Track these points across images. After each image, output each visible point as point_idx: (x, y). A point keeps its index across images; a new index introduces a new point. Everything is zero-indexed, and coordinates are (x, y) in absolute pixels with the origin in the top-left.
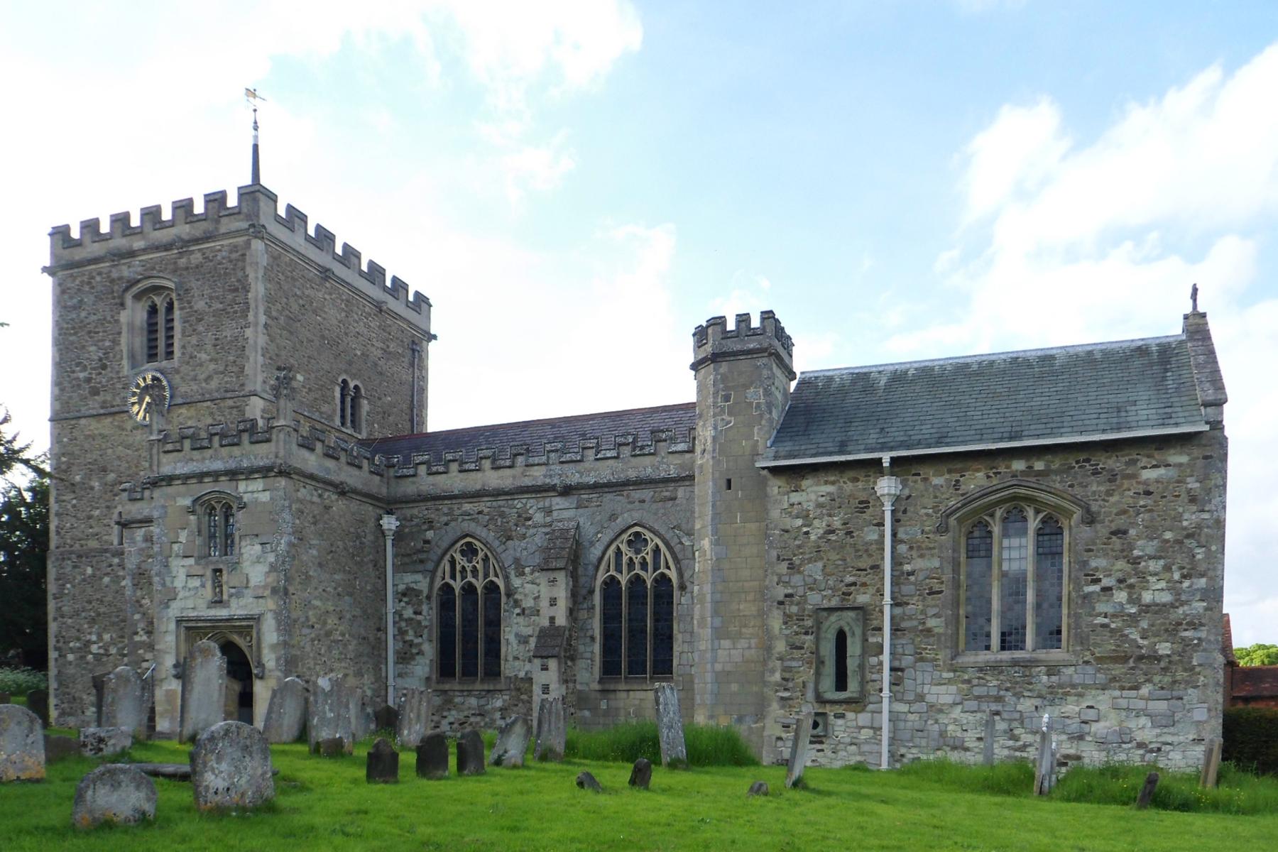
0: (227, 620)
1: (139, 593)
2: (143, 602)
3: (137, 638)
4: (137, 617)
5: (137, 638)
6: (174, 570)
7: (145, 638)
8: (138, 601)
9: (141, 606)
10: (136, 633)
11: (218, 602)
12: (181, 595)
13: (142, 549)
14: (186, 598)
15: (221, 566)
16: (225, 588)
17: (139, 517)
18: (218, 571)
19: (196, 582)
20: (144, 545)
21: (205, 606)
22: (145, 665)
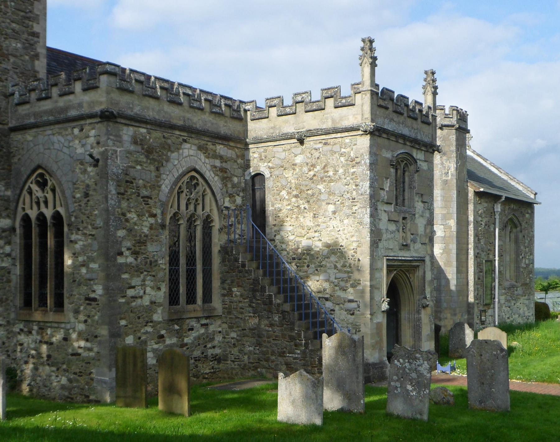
0: (410, 261)
1: (124, 204)
2: (129, 215)
3: (121, 260)
4: (121, 233)
5: (121, 260)
6: (379, 211)
7: (130, 260)
8: (124, 214)
9: (127, 220)
10: (121, 254)
11: (405, 247)
12: (384, 237)
13: (129, 152)
14: (389, 239)
15: (407, 216)
16: (409, 234)
17: (129, 113)
18: (404, 218)
19: (392, 227)
20: (132, 148)
21: (397, 247)
22: (131, 293)
